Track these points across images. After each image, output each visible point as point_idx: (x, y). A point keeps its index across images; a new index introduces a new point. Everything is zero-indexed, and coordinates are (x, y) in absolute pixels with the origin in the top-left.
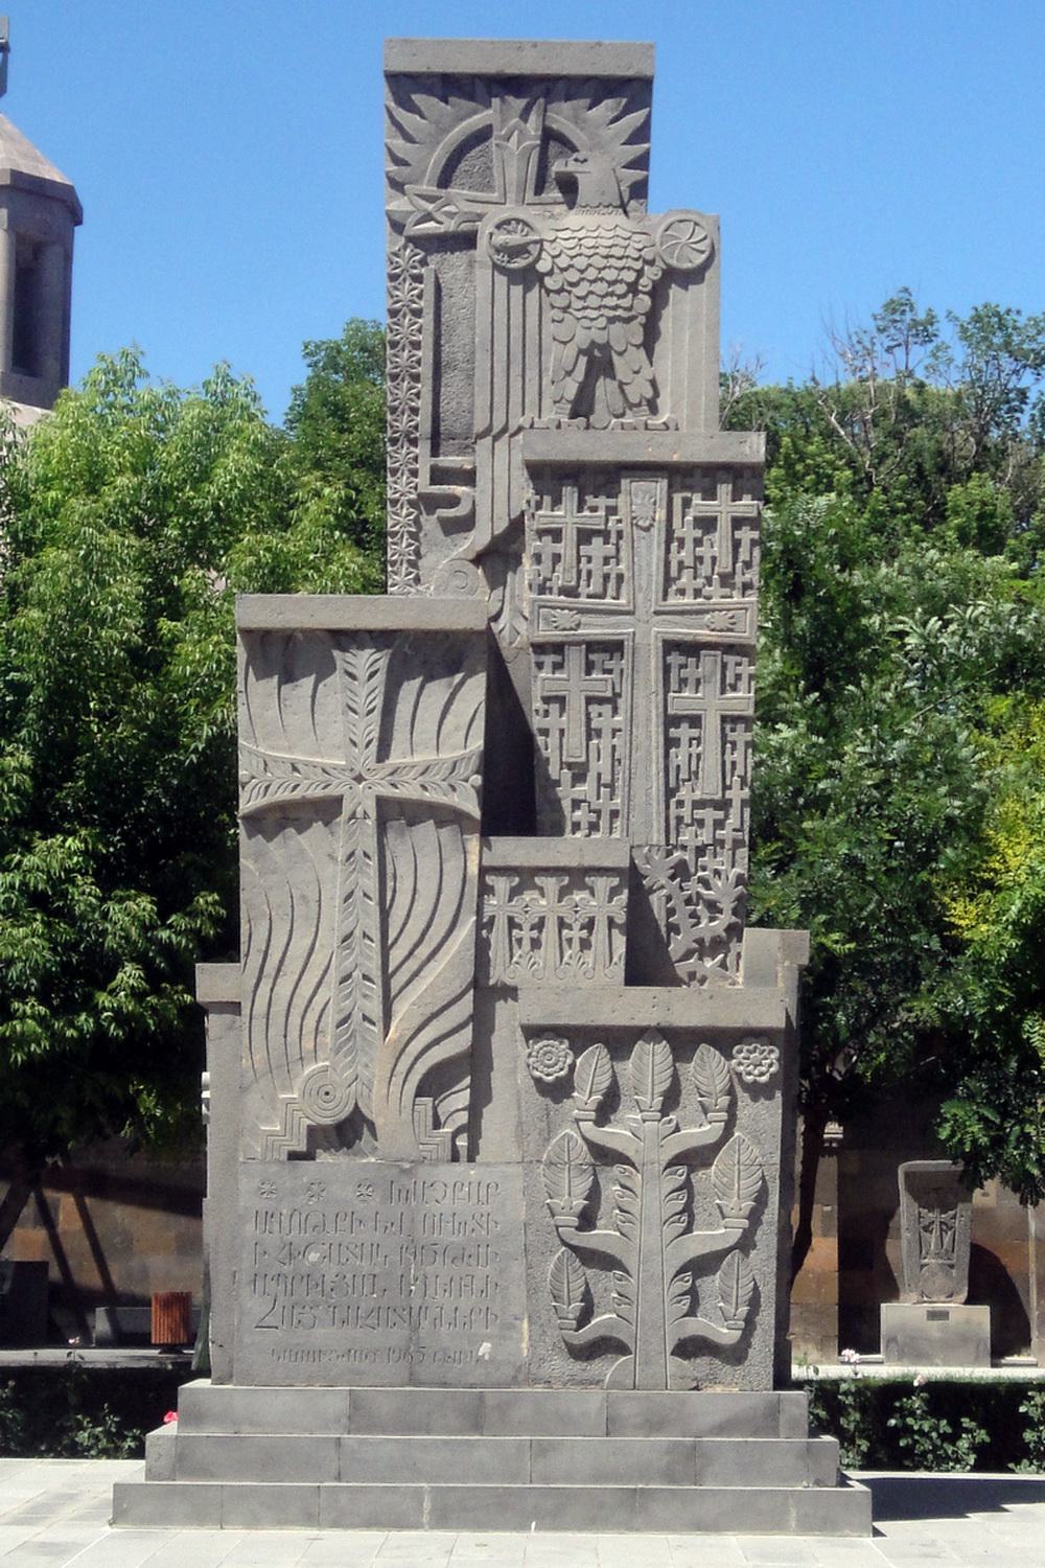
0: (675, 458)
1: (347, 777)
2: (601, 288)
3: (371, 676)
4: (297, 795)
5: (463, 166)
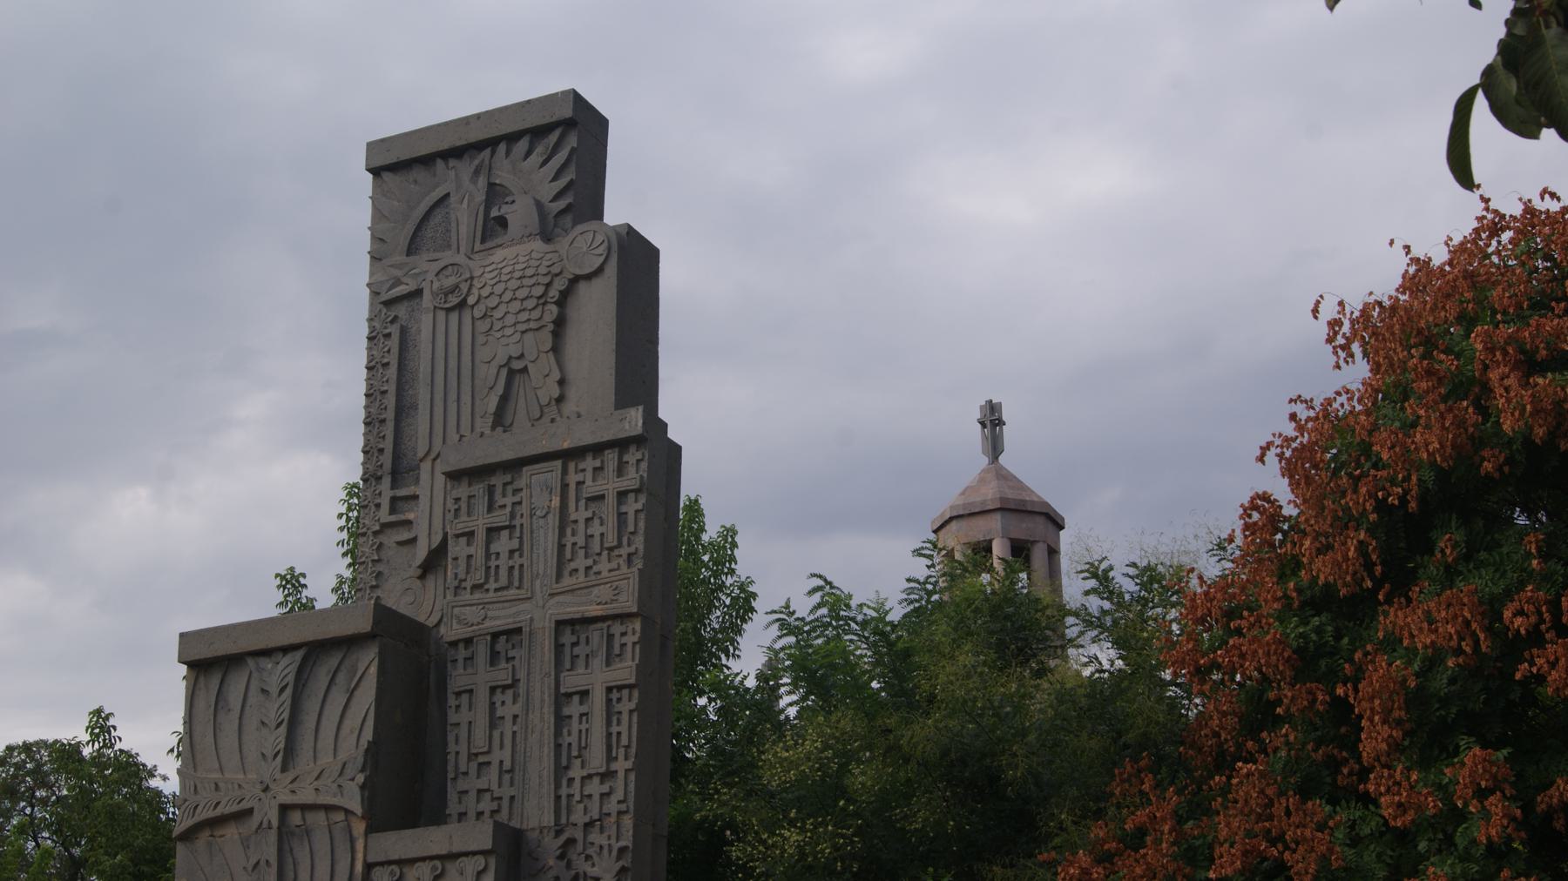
0: (566, 445)
1: (258, 789)
2: (516, 306)
3: (282, 690)
4: (218, 812)
5: (428, 232)
